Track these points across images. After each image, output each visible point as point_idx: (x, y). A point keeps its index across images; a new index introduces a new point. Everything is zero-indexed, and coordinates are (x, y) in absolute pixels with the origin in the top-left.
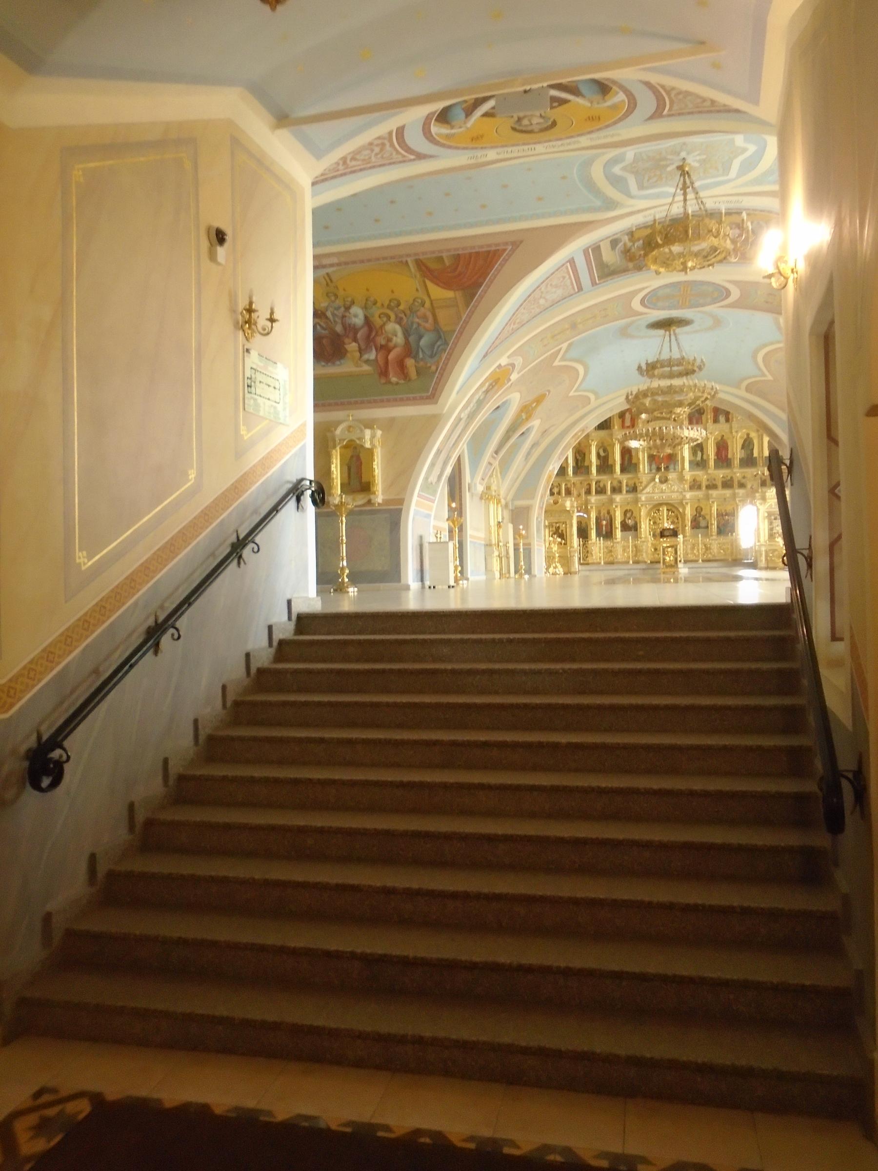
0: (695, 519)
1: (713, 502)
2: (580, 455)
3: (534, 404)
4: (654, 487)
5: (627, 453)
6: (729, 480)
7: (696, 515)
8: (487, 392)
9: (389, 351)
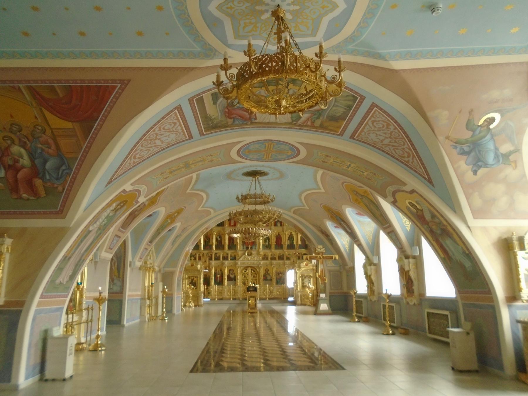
1: (274, 267)
2: (208, 238)
3: (176, 214)
4: (245, 258)
5: (231, 239)
6: (282, 256)
8: (116, 210)
9: (18, 171)
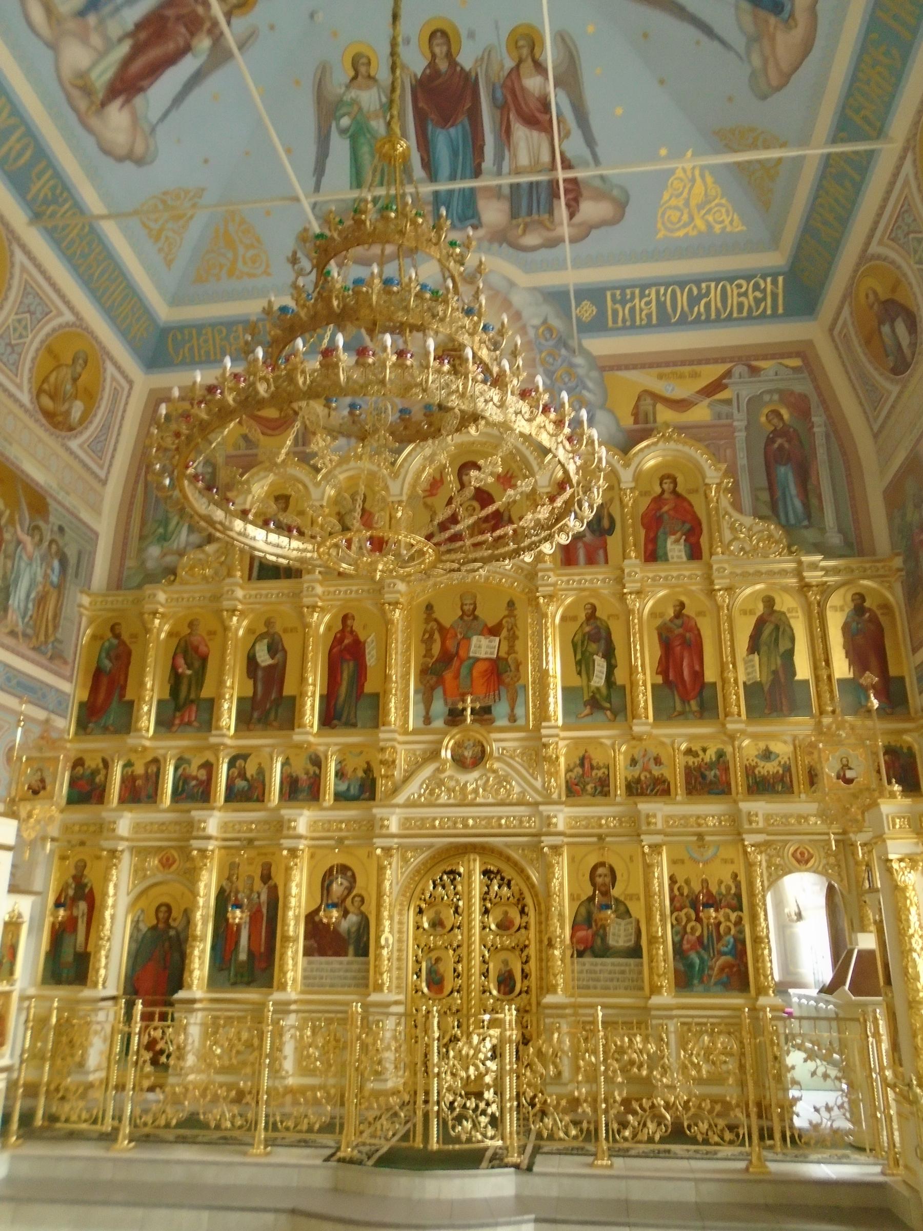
0: (589, 914)
1: (656, 848)
4: (436, 782)
6: (710, 766)
7: (591, 899)
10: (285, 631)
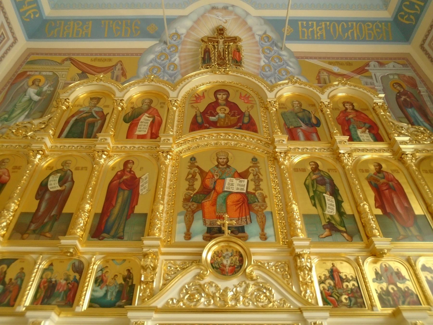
10: (77, 169)
